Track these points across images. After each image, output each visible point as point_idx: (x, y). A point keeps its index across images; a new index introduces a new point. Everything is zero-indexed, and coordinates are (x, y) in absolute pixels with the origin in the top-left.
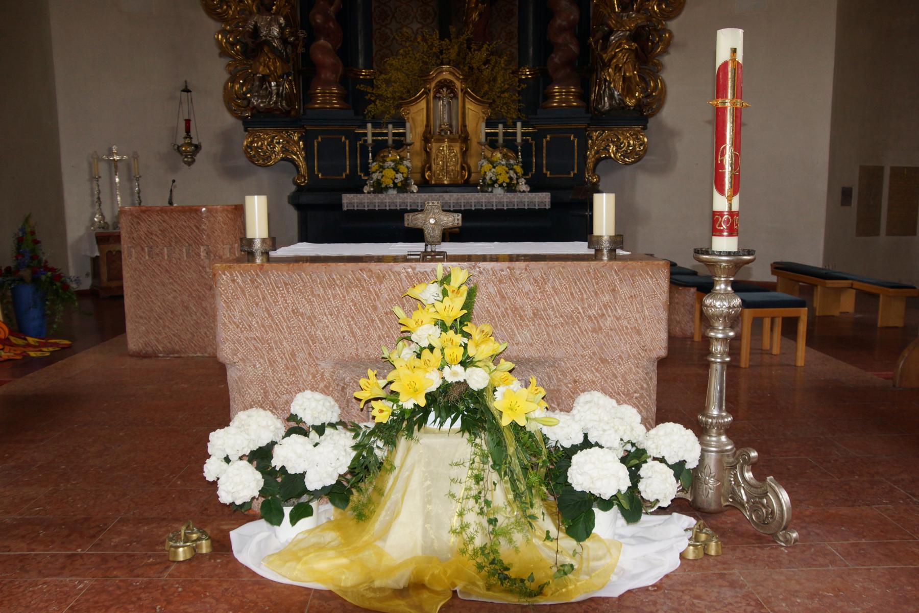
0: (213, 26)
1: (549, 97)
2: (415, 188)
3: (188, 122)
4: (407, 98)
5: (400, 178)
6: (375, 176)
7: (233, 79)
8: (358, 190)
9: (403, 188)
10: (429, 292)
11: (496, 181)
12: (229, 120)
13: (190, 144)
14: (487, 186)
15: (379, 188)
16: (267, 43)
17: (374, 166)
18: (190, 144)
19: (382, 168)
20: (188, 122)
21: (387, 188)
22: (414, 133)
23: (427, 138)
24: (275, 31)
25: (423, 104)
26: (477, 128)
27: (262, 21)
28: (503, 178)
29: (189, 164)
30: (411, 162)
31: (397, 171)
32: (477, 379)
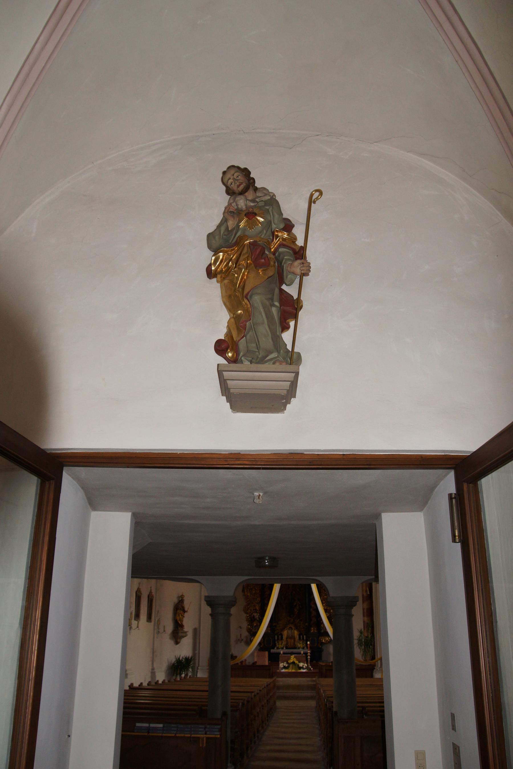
0: (245, 615)
1: (311, 630)
2: (285, 648)
3: (241, 634)
4: (283, 629)
5: (282, 646)
6: (277, 646)
7: (249, 625)
8: (274, 649)
9: (282, 648)
10: (292, 656)
11: (300, 647)
12: (247, 634)
13: (241, 639)
14: (299, 648)
15: (278, 648)
16: (256, 619)
17: (277, 644)
18: (241, 639)
19: (279, 644)
20: (241, 634)
21: (280, 648)
22: (284, 637)
23: (287, 638)
24: (257, 616)
25: (286, 631)
26: (297, 637)
27: (255, 614)
28: (302, 647)
29: (241, 643)
30: (284, 643)
31: (281, 645)
32: (294, 661)
